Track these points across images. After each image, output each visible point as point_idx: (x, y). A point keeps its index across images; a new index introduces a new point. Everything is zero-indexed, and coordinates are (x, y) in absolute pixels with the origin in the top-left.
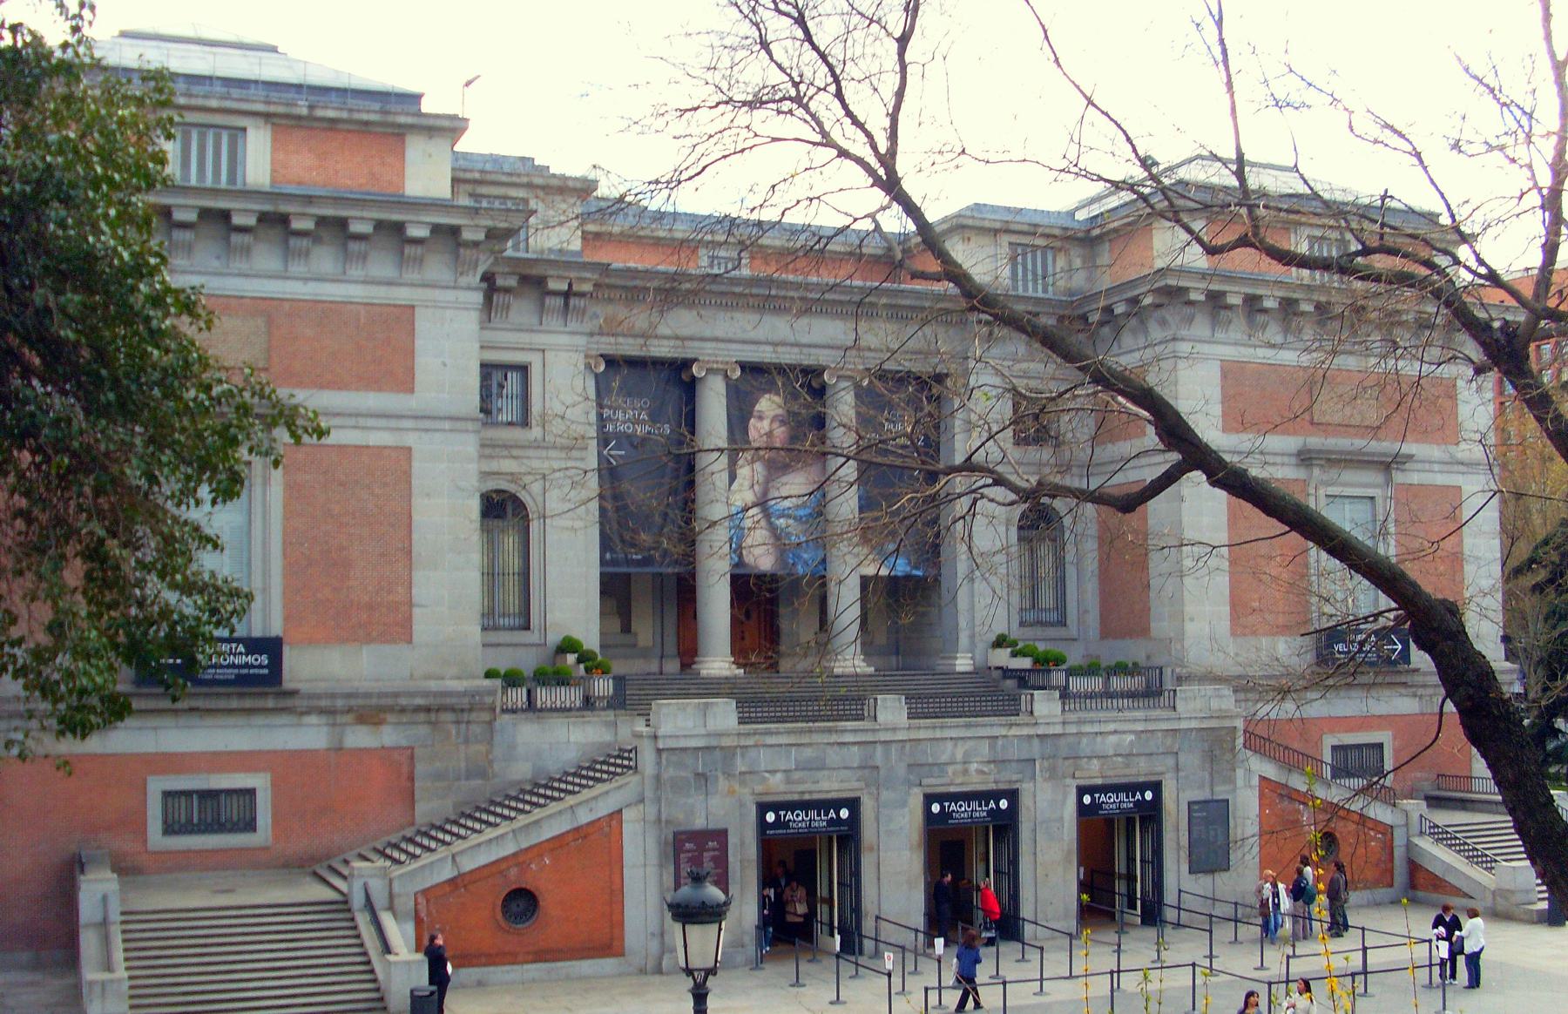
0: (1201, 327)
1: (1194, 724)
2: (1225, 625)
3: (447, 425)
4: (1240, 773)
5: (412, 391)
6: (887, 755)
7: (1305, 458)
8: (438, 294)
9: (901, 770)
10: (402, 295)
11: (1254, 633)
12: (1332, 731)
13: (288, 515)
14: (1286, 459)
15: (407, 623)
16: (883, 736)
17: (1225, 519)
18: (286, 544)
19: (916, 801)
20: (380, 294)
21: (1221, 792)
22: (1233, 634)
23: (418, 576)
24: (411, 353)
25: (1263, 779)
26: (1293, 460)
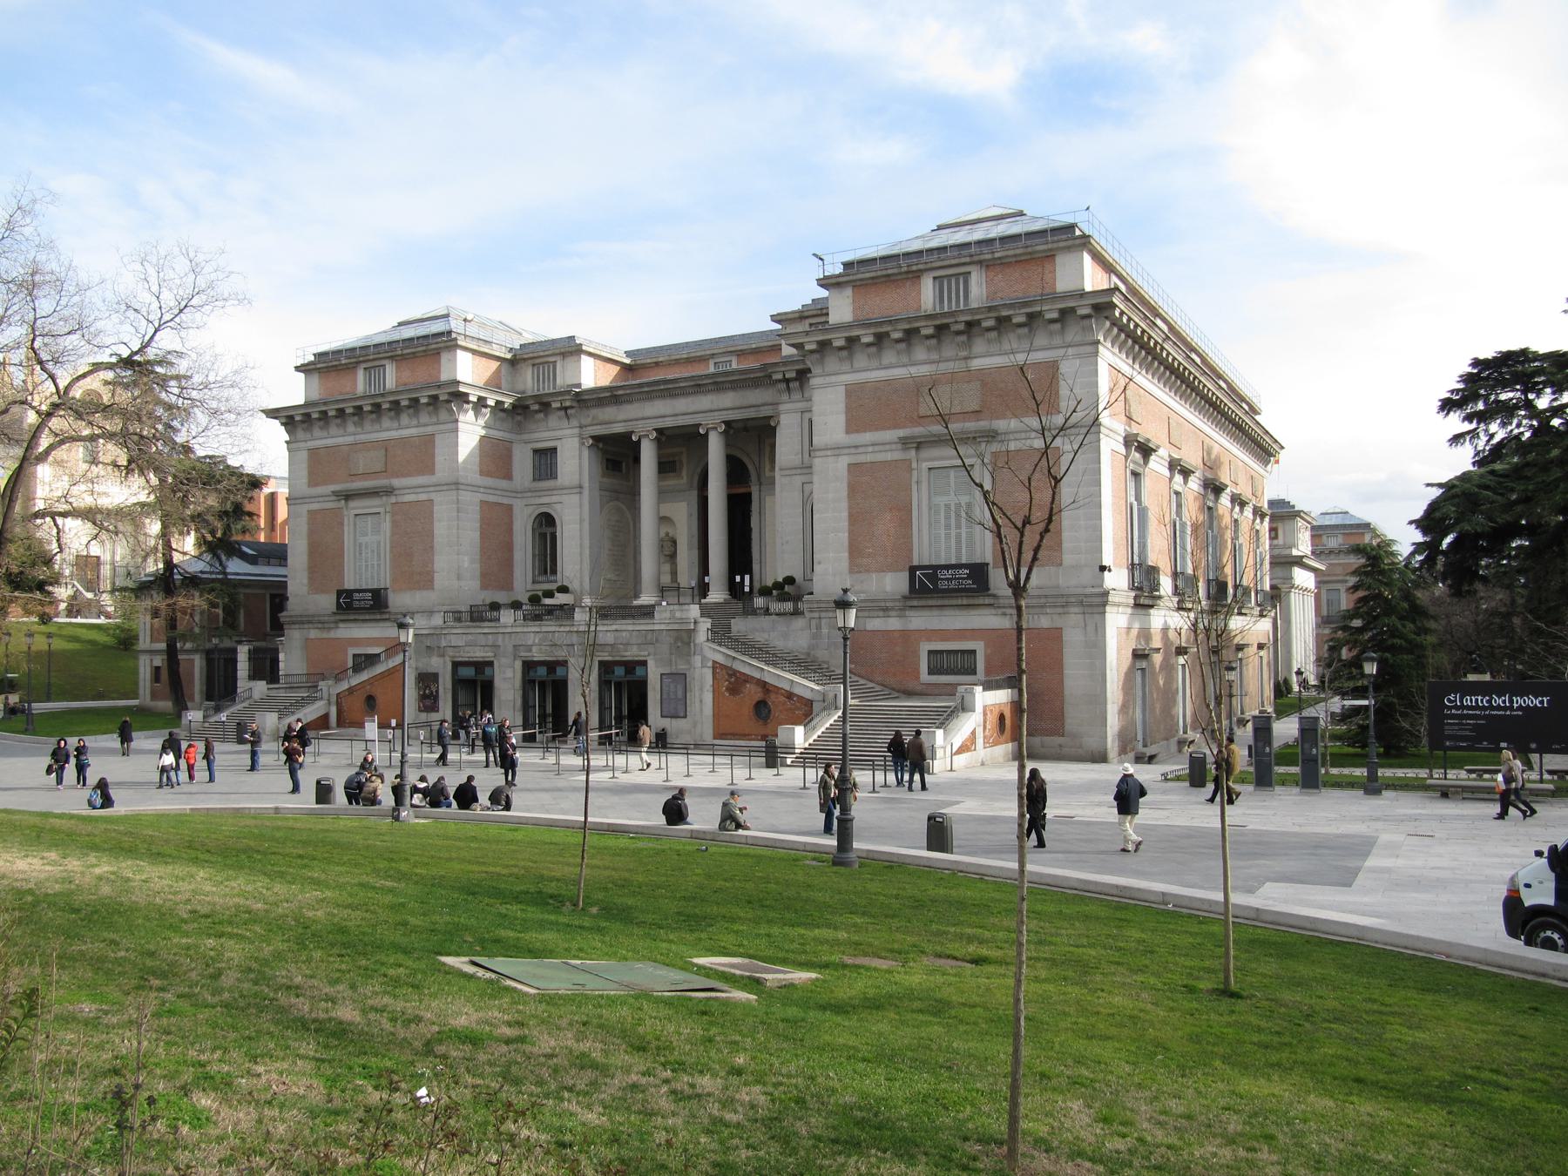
0: (832, 363)
1: (663, 627)
2: (845, 564)
3: (445, 488)
4: (697, 660)
5: (433, 474)
6: (503, 640)
7: (905, 442)
8: (442, 427)
9: (510, 649)
10: (429, 429)
11: (868, 571)
12: (929, 640)
13: (393, 534)
14: (894, 446)
15: (432, 581)
16: (501, 630)
17: (846, 493)
18: (391, 547)
19: (518, 665)
20: (422, 430)
21: (682, 667)
22: (851, 571)
23: (436, 558)
24: (433, 456)
25: (714, 662)
26: (899, 446)
